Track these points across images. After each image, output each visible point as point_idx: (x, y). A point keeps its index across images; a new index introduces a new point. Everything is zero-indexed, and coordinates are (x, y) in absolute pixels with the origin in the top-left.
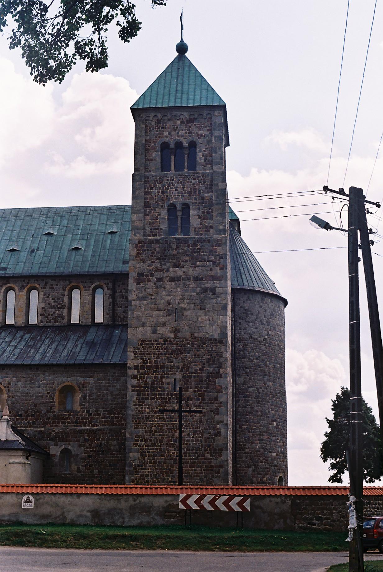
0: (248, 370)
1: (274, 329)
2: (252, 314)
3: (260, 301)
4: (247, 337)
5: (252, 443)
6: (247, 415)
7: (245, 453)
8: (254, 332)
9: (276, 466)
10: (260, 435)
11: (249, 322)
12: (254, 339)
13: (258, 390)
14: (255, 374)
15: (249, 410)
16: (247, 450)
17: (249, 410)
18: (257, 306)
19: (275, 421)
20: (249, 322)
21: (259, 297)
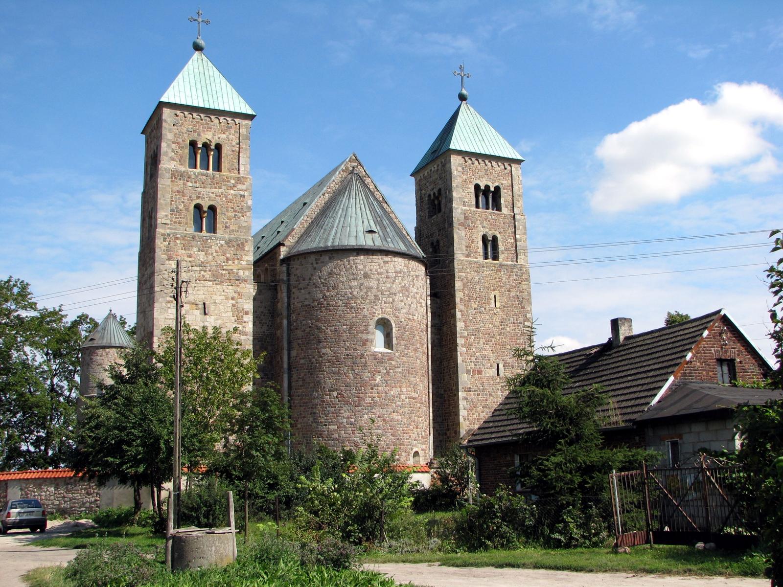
0: (300, 341)
1: (336, 287)
2: (304, 280)
3: (314, 264)
4: (299, 305)
5: (304, 417)
6: (299, 389)
7: (298, 429)
8: (306, 299)
9: (337, 439)
10: (312, 408)
11: (301, 289)
12: (306, 305)
13: (310, 361)
14: (307, 343)
15: (301, 383)
16: (299, 426)
17: (301, 383)
18: (310, 269)
19: (336, 390)
20: (301, 289)
21: (312, 258)
